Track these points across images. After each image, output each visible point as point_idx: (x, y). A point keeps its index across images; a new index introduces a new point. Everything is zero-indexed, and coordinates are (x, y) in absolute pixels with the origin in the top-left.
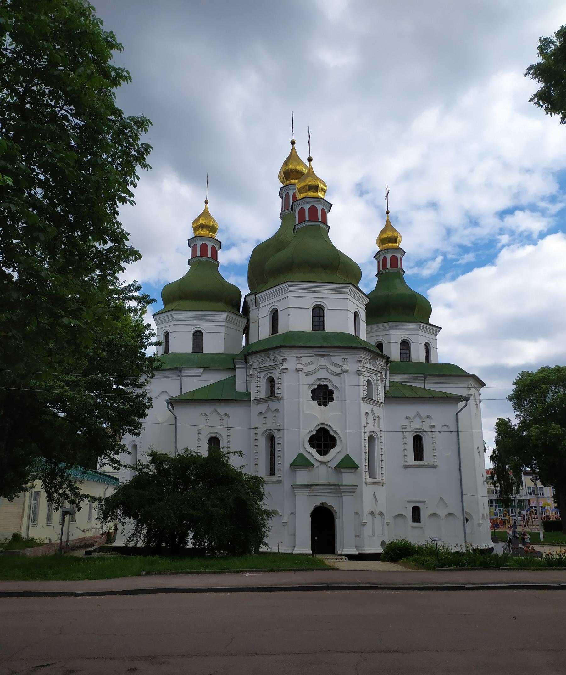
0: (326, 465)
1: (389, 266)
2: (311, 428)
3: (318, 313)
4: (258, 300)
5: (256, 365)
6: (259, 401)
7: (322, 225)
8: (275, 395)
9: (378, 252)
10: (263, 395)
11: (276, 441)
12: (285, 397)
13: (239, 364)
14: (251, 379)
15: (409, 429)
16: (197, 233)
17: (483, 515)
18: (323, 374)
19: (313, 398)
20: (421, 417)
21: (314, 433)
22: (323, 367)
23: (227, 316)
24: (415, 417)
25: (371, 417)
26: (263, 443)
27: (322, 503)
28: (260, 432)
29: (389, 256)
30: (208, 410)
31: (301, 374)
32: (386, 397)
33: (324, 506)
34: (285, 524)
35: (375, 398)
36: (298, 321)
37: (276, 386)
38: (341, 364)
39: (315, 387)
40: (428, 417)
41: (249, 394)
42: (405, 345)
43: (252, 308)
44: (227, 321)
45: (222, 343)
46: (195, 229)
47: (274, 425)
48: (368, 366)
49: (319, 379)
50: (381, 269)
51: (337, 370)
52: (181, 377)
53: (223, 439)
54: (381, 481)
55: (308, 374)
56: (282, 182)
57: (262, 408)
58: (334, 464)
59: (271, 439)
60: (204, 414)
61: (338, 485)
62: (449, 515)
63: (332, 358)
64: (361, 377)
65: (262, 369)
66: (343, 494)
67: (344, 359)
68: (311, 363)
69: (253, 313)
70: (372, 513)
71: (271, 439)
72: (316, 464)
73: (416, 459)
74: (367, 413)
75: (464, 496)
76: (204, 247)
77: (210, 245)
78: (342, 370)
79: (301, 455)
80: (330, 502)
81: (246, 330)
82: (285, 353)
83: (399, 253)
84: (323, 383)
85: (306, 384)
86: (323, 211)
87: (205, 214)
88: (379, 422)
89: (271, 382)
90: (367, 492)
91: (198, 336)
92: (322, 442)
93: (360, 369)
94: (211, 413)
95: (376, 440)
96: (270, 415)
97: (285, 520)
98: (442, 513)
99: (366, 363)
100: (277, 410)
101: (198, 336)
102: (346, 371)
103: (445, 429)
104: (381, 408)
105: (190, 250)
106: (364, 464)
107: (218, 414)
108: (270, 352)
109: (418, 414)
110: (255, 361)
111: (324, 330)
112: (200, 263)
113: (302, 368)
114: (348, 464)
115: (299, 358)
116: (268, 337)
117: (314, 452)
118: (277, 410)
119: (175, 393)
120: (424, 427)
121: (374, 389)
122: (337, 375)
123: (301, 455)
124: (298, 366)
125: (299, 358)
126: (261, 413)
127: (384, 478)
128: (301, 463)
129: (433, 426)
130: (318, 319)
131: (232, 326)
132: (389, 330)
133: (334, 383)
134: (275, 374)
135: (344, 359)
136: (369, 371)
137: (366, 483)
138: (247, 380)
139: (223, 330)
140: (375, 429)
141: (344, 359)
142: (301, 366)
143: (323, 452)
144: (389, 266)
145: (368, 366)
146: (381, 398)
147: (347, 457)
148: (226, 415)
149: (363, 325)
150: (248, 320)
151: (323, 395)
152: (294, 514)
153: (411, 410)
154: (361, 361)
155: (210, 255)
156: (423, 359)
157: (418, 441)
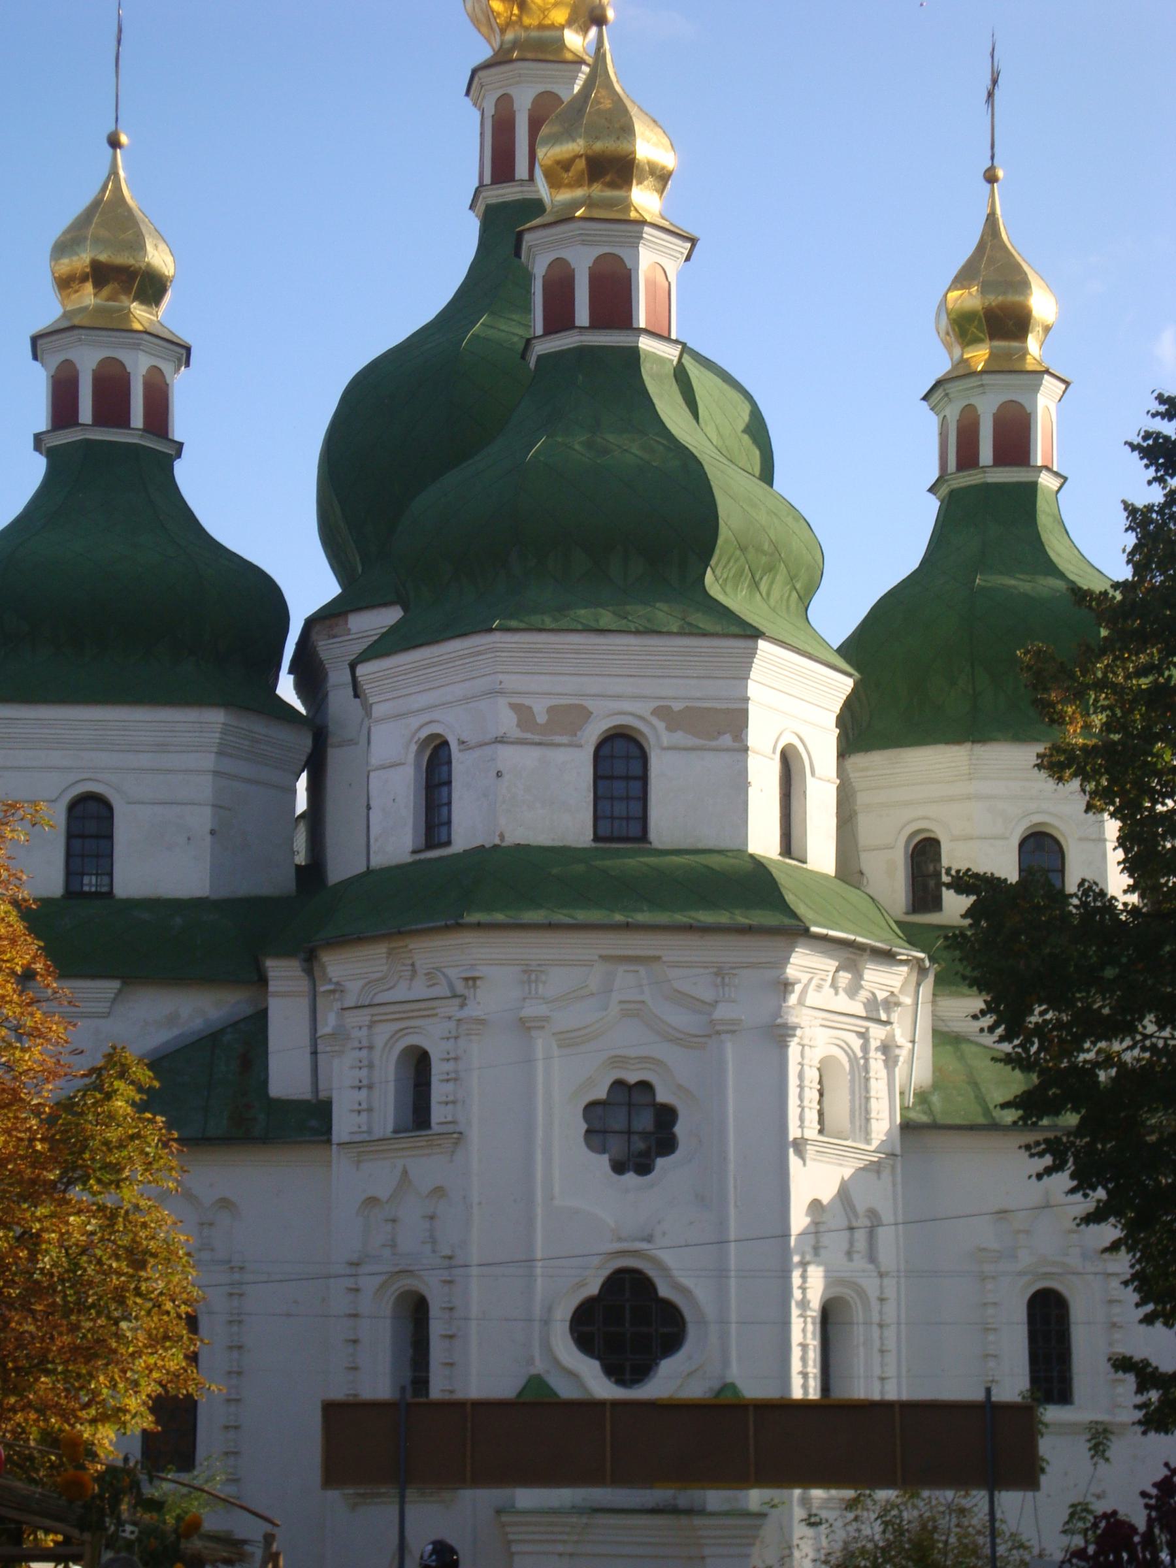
3: (621, 765)
4: (366, 687)
6: (363, 1147)
8: (435, 1128)
11: (436, 1328)
12: (475, 1136)
13: (283, 974)
21: (593, 1289)
29: (986, 410)
36: (537, 800)
37: (439, 1091)
39: (601, 1093)
43: (338, 677)
46: (65, 283)
49: (618, 1061)
55: (569, 1040)
57: (379, 1176)
66: (707, 1551)
77: (139, 365)
84: (632, 1078)
85: (564, 1087)
89: (418, 1064)
95: (859, 1315)
111: (643, 837)
113: (546, 1019)
118: (439, 1192)
126: (372, 1201)
130: (619, 787)
138: (315, 1053)
139: (204, 787)
142: (542, 1010)
148: (225, 1204)
155: (137, 418)
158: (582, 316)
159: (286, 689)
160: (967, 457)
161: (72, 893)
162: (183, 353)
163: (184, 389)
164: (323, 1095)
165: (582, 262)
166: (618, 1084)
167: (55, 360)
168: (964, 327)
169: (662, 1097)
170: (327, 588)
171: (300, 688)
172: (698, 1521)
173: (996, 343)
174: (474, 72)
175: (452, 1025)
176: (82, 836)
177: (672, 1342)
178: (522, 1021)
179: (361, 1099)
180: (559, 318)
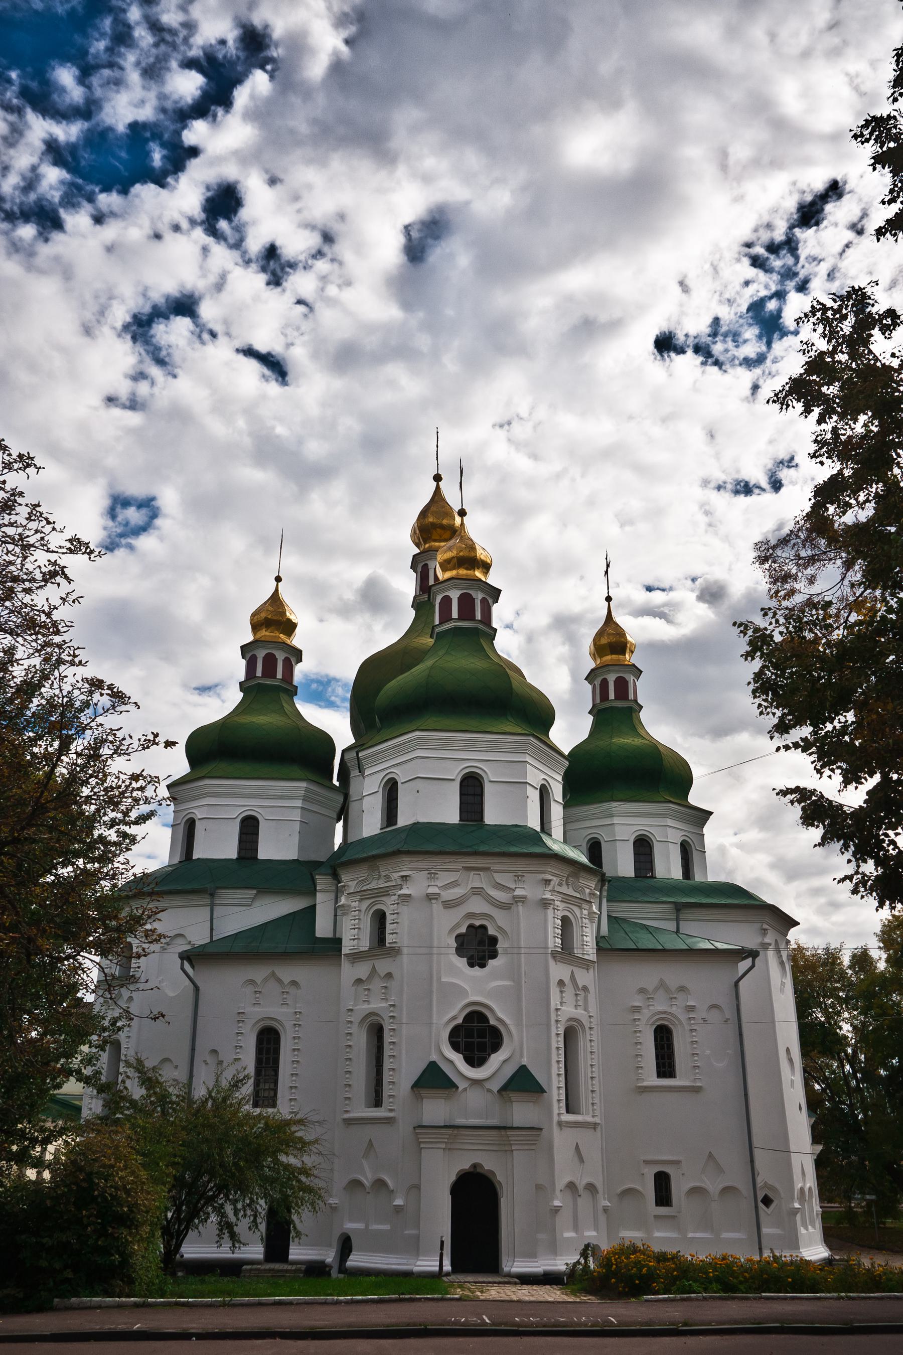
0: (483, 1087)
1: (612, 696)
2: (453, 1013)
3: (472, 788)
5: (352, 886)
6: (356, 957)
7: (481, 626)
8: (387, 945)
9: (592, 670)
10: (365, 944)
11: (387, 1038)
13: (322, 881)
14: (344, 914)
15: (646, 1013)
16: (258, 636)
17: (802, 1189)
18: (477, 906)
20: (667, 990)
21: (460, 1021)
22: (477, 892)
24: (656, 989)
26: (361, 1040)
27: (475, 1166)
28: (356, 1018)
29: (611, 678)
30: (259, 973)
31: (437, 907)
32: (599, 949)
33: (479, 1170)
34: (398, 1209)
35: (577, 952)
37: (389, 928)
38: (513, 886)
39: (463, 930)
40: (682, 989)
42: (643, 848)
43: (354, 773)
44: (305, 799)
46: (255, 627)
47: (384, 1005)
48: (564, 889)
50: (598, 701)
52: (212, 906)
53: (285, 1032)
55: (449, 905)
56: (418, 545)
57: (362, 970)
58: (496, 1086)
59: (377, 1032)
60: (252, 982)
61: (505, 1128)
62: (727, 1190)
63: (495, 875)
64: (550, 912)
65: (363, 895)
67: (518, 876)
68: (454, 884)
70: (571, 1186)
71: (377, 1032)
72: (462, 1085)
73: (661, 1074)
74: (561, 983)
75: (756, 1152)
76: (270, 661)
78: (514, 897)
79: (433, 1066)
80: (489, 1163)
81: (343, 813)
82: (405, 867)
83: (630, 672)
84: (477, 923)
85: (446, 926)
86: (484, 601)
87: (275, 598)
88: (586, 999)
89: (380, 919)
90: (562, 1143)
91: (249, 828)
92: (476, 1040)
93: (548, 896)
94: (265, 980)
96: (376, 985)
97: (399, 1202)
98: (713, 1186)
99: (560, 884)
100: (389, 975)
101: (249, 828)
102: (522, 900)
103: (715, 1013)
104: (591, 971)
106: (555, 1084)
107: (279, 981)
109: (662, 985)
110: (350, 880)
113: (439, 894)
114: (523, 1083)
115: (432, 876)
116: (378, 831)
117: (457, 1059)
118: (389, 975)
119: (199, 936)
120: (674, 1010)
123: (433, 1066)
124: (431, 890)
125: (432, 876)
126: (359, 981)
127: (597, 1113)
128: (433, 1079)
129: (691, 1009)
131: (315, 808)
132: (612, 816)
133: (498, 923)
134: (388, 905)
135: (519, 878)
136: (566, 899)
137: (560, 1124)
138: (336, 916)
139: (297, 816)
140: (580, 1013)
141: (519, 878)
143: (475, 1059)
144: (612, 696)
145: (564, 889)
146: (590, 951)
148: (294, 983)
149: (557, 812)
150: (346, 796)
151: (478, 946)
152: (417, 1187)
153: (648, 974)
154: (550, 881)
155: (279, 675)
156: (677, 873)
157: (663, 1037)
158: (455, 615)
161: (240, 858)
164: (337, 936)
167: (248, 656)
169: (491, 931)
170: (350, 740)
172: (510, 1133)
173: (613, 656)
174: (414, 556)
175: (396, 897)
176: (247, 834)
177: (496, 1045)
178: (428, 895)
179: (355, 935)
180: (446, 616)
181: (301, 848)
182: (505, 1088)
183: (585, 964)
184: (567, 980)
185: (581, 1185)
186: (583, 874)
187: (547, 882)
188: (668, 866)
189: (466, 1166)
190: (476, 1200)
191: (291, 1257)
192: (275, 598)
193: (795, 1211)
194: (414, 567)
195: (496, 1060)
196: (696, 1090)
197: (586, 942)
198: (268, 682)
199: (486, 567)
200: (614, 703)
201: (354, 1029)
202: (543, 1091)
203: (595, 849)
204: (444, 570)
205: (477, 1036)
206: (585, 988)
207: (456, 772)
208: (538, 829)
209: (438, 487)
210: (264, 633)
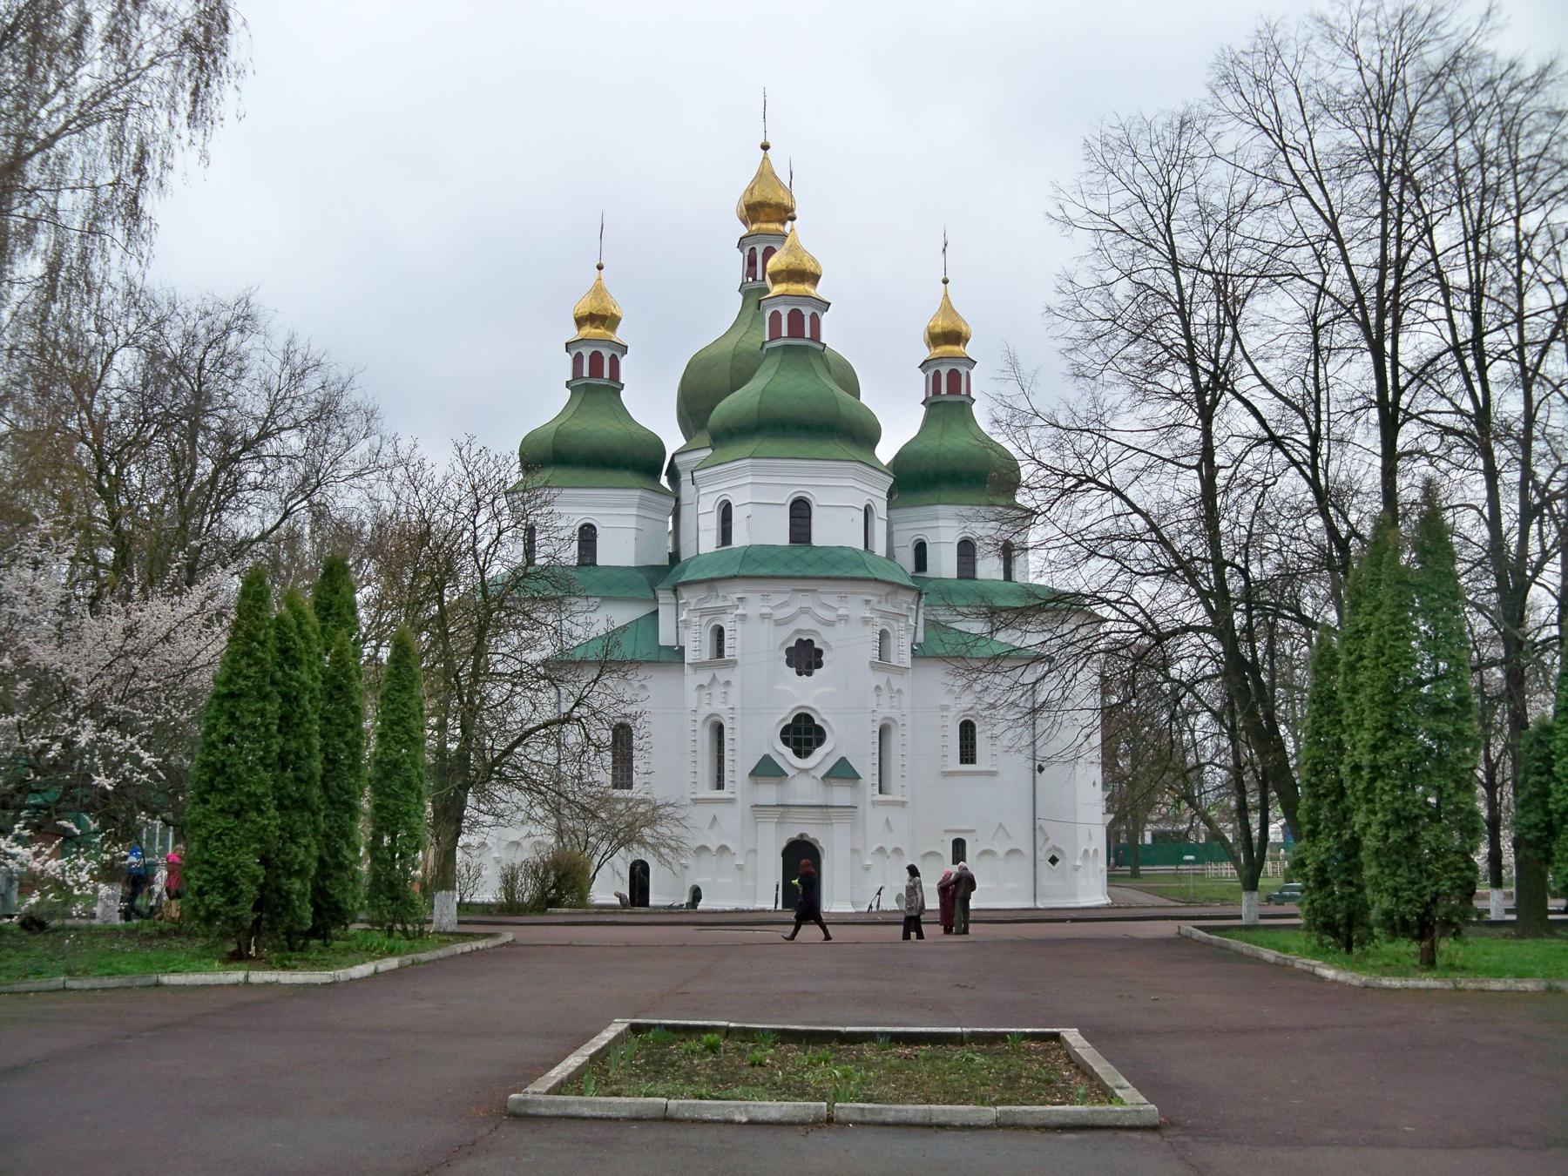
1: (944, 391)
2: (785, 716)
3: (800, 511)
6: (698, 666)
10: (706, 655)
13: (664, 597)
17: (1086, 851)
18: (805, 623)
19: (789, 663)
23: (641, 498)
25: (885, 694)
26: (705, 737)
28: (700, 718)
29: (944, 371)
34: (740, 868)
35: (894, 662)
37: (727, 643)
41: (682, 649)
43: (685, 477)
45: (632, 546)
46: (580, 321)
49: (799, 631)
51: (828, 615)
54: (899, 798)
55: (780, 623)
56: (745, 223)
57: (704, 677)
59: (719, 730)
65: (703, 613)
68: (785, 604)
69: (687, 489)
70: (881, 850)
74: (878, 688)
76: (596, 358)
80: (813, 833)
87: (598, 291)
89: (719, 632)
90: (874, 818)
93: (868, 614)
96: (718, 690)
98: (1001, 848)
100: (728, 683)
102: (845, 618)
105: (568, 359)
108: (719, 585)
111: (809, 540)
112: (588, 388)
114: (843, 772)
115: (766, 597)
117: (788, 752)
118: (728, 683)
121: (893, 641)
122: (830, 624)
126: (701, 686)
128: (766, 770)
130: (799, 521)
132: (937, 519)
133: (823, 638)
134: (727, 623)
136: (885, 615)
137: (873, 803)
139: (632, 522)
142: (766, 610)
143: (802, 750)
144: (944, 391)
147: (843, 759)
150: (677, 500)
152: (755, 851)
155: (606, 375)
158: (785, 333)
159: (664, 481)
160: (937, 391)
162: (624, 349)
163: (624, 362)
165: (784, 311)
166: (799, 641)
167: (574, 353)
168: (936, 339)
171: (669, 481)
177: (820, 742)
179: (697, 646)
180: (775, 334)
181: (637, 556)
182: (828, 776)
183: (901, 670)
184: (883, 684)
185: (889, 848)
186: (901, 591)
187: (868, 602)
188: (989, 568)
189: (795, 835)
190: (802, 861)
191: (651, 903)
192: (598, 291)
193: (1076, 868)
194: (741, 245)
195: (819, 753)
196: (993, 774)
197: (901, 651)
198: (595, 381)
199: (814, 278)
200: (947, 397)
201: (698, 727)
202: (858, 777)
203: (920, 549)
204: (774, 282)
205: (803, 733)
206: (899, 691)
207: (786, 497)
208: (862, 547)
209: (765, 158)
210: (589, 331)
